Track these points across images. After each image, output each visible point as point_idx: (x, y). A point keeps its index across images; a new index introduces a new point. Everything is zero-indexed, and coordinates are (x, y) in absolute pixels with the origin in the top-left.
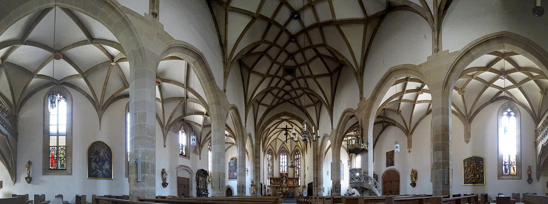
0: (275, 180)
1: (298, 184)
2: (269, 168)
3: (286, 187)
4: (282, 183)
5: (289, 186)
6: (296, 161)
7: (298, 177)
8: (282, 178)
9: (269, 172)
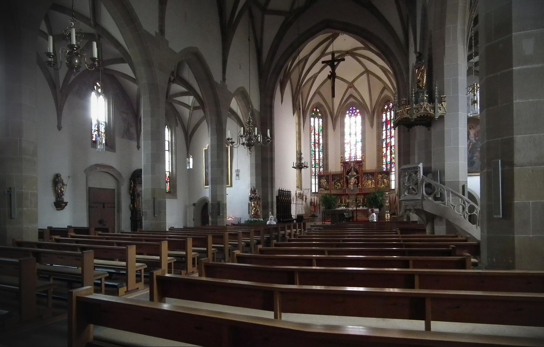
0: (331, 179)
1: (389, 185)
2: (317, 150)
3: (358, 194)
5: (364, 192)
6: (384, 129)
7: (388, 167)
8: (348, 173)
9: (317, 161)
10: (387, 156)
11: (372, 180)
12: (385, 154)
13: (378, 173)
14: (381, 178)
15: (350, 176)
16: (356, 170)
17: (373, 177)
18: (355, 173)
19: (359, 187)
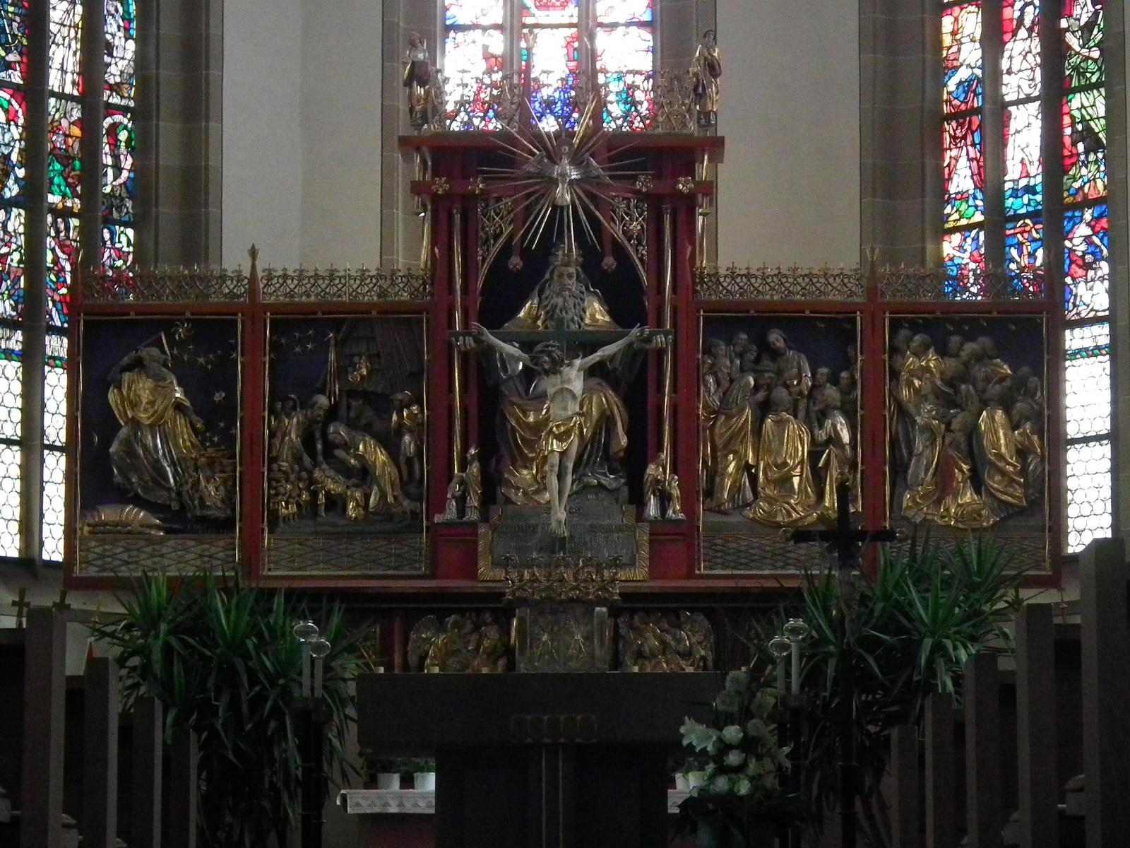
4: (491, 485)
10: (1000, 113)
11: (823, 415)
12: (966, 86)
13: (895, 326)
14: (938, 394)
15: (527, 346)
16: (609, 262)
17: (834, 380)
18: (596, 313)
19: (652, 509)
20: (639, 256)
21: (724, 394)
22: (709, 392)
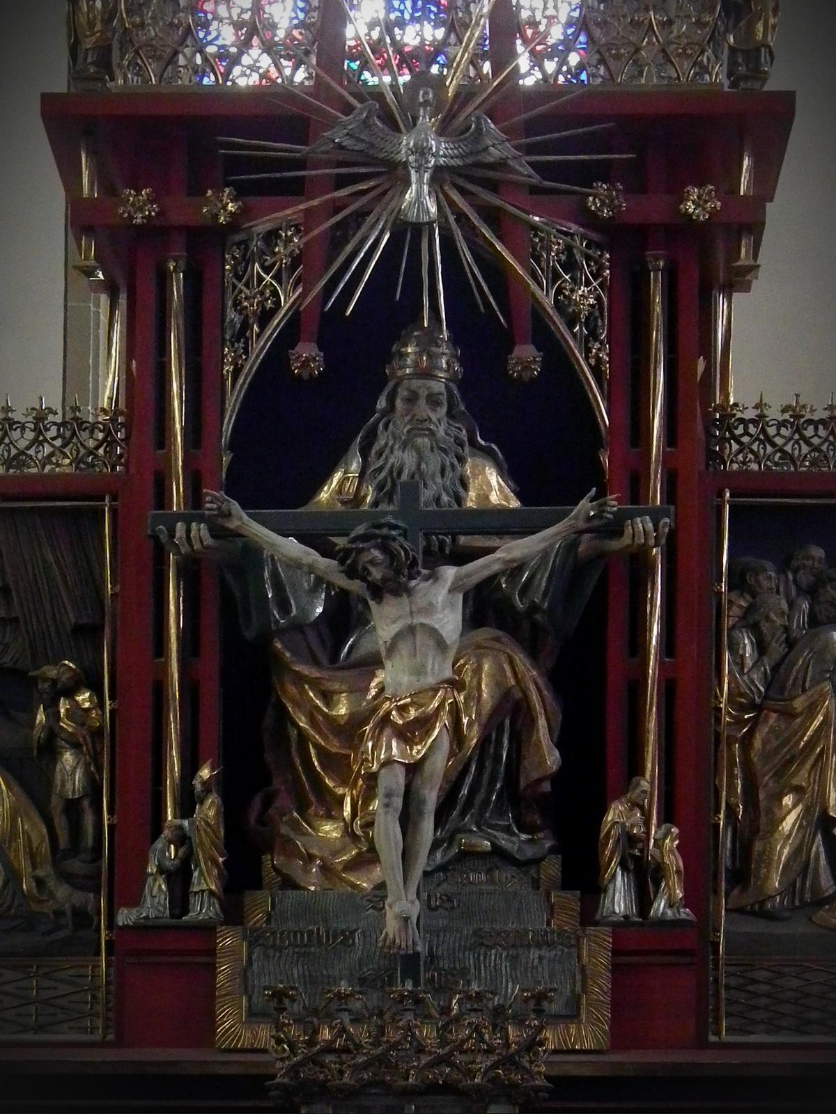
16: (526, 357)
20: (593, 362)
21: (775, 669)
22: (742, 665)
